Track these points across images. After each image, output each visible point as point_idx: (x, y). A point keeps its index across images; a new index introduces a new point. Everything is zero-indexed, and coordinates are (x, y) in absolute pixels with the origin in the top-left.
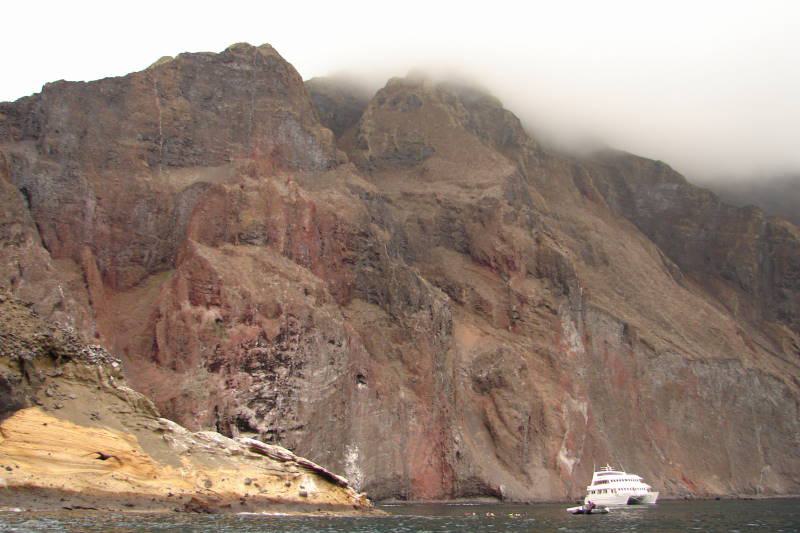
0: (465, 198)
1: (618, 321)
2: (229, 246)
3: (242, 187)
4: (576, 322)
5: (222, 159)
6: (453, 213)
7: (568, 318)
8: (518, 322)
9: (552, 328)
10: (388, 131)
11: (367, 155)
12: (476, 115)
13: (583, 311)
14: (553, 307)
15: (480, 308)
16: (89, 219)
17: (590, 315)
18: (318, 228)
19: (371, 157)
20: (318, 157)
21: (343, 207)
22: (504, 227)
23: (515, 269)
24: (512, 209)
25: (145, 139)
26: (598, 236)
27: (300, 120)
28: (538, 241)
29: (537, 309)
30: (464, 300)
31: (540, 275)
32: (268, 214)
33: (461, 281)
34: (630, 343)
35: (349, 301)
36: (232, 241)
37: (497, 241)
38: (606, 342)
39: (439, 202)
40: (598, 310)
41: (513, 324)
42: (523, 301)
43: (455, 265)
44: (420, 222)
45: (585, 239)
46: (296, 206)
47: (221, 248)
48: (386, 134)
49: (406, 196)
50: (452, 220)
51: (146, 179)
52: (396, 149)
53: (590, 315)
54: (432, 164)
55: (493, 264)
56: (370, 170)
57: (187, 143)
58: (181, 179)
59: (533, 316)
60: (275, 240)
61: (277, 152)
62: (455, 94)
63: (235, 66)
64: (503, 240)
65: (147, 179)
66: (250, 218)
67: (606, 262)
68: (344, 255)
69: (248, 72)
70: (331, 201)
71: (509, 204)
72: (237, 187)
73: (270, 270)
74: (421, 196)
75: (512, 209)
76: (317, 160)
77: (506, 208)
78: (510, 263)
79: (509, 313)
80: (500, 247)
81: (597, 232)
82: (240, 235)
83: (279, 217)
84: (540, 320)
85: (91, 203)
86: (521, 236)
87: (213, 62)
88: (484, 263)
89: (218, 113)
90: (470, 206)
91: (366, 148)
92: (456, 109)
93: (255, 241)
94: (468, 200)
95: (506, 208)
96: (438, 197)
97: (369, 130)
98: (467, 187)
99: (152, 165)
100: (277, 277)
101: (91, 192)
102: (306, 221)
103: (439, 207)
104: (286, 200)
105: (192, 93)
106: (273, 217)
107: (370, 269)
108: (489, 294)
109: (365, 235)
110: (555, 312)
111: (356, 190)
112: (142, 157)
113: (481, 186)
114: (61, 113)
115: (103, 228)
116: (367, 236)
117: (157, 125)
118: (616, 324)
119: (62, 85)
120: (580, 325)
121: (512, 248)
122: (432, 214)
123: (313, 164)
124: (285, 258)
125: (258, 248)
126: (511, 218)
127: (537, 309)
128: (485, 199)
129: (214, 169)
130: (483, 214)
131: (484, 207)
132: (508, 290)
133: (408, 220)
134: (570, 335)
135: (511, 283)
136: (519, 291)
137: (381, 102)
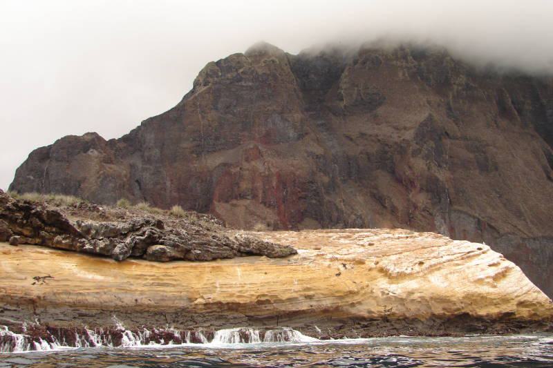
0: (395, 137)
1: (474, 217)
2: (234, 202)
3: (241, 169)
4: (445, 219)
5: (236, 143)
6: (386, 148)
7: (439, 218)
8: (412, 220)
9: (429, 224)
10: (357, 86)
11: (342, 104)
12: (422, 64)
13: (449, 215)
14: (431, 211)
15: (394, 210)
16: (168, 191)
17: (453, 215)
18: (283, 182)
19: (345, 106)
20: (292, 134)
21: (299, 168)
22: (411, 159)
23: (415, 187)
24: (418, 147)
25: (194, 140)
26: (495, 150)
27: (281, 113)
28: (429, 169)
29: (423, 213)
30: (386, 205)
31: (428, 191)
32: (253, 183)
33: (385, 194)
34: (481, 231)
35: (302, 220)
36: (236, 198)
37: (406, 168)
38: (465, 230)
39: (379, 140)
40: (461, 212)
41: (410, 220)
42: (416, 207)
43: (384, 181)
44: (367, 154)
45: (484, 153)
46: (268, 176)
47: (230, 203)
48: (356, 88)
49: (362, 135)
50: (386, 152)
51: (196, 166)
52: (362, 99)
53: (453, 215)
54: (380, 111)
55: (404, 183)
56: (345, 115)
57: (217, 139)
58: (213, 161)
59: (419, 217)
60: (257, 196)
61: (268, 135)
62: (408, 50)
63: (243, 83)
64: (410, 168)
65: (196, 165)
66: (244, 186)
67: (496, 169)
68: (300, 195)
69: (250, 86)
70: (293, 166)
71: (417, 143)
72: (238, 169)
73: (252, 214)
74: (371, 135)
75: (418, 147)
76: (291, 135)
77: (414, 146)
78: (412, 183)
79: (409, 214)
80: (408, 173)
81: (495, 147)
82: (240, 195)
83: (259, 184)
84: (423, 219)
85: (168, 184)
86: (419, 164)
87: (231, 83)
88: (399, 181)
89: (234, 115)
90: (396, 143)
91: (342, 100)
92: (407, 62)
93: (248, 197)
94: (396, 140)
95: (414, 146)
96: (379, 138)
97: (344, 86)
98: (398, 129)
99: (199, 154)
100: (256, 217)
101: (168, 178)
102: (274, 184)
103: (379, 144)
104: (263, 174)
105: (219, 106)
106: (255, 185)
107: (314, 201)
108: (399, 203)
109: (312, 182)
110: (431, 214)
111: (310, 154)
112: (192, 152)
113: (405, 128)
114: (150, 137)
115: (175, 194)
116: (313, 183)
117: (200, 132)
118: (472, 219)
119: (151, 119)
120: (448, 221)
121: (414, 173)
122: (374, 149)
123: (289, 138)
124: (262, 206)
125: (248, 201)
126: (415, 154)
127: (423, 213)
128: (404, 140)
129: (231, 151)
130: (401, 149)
131: (403, 145)
132: (409, 200)
133: (361, 153)
134: (440, 227)
135: (410, 196)
136: (414, 201)
137: (355, 62)
